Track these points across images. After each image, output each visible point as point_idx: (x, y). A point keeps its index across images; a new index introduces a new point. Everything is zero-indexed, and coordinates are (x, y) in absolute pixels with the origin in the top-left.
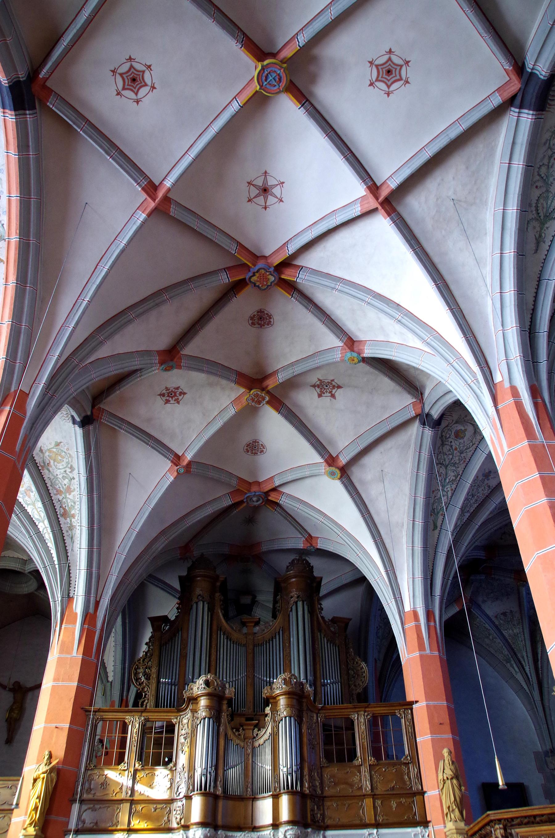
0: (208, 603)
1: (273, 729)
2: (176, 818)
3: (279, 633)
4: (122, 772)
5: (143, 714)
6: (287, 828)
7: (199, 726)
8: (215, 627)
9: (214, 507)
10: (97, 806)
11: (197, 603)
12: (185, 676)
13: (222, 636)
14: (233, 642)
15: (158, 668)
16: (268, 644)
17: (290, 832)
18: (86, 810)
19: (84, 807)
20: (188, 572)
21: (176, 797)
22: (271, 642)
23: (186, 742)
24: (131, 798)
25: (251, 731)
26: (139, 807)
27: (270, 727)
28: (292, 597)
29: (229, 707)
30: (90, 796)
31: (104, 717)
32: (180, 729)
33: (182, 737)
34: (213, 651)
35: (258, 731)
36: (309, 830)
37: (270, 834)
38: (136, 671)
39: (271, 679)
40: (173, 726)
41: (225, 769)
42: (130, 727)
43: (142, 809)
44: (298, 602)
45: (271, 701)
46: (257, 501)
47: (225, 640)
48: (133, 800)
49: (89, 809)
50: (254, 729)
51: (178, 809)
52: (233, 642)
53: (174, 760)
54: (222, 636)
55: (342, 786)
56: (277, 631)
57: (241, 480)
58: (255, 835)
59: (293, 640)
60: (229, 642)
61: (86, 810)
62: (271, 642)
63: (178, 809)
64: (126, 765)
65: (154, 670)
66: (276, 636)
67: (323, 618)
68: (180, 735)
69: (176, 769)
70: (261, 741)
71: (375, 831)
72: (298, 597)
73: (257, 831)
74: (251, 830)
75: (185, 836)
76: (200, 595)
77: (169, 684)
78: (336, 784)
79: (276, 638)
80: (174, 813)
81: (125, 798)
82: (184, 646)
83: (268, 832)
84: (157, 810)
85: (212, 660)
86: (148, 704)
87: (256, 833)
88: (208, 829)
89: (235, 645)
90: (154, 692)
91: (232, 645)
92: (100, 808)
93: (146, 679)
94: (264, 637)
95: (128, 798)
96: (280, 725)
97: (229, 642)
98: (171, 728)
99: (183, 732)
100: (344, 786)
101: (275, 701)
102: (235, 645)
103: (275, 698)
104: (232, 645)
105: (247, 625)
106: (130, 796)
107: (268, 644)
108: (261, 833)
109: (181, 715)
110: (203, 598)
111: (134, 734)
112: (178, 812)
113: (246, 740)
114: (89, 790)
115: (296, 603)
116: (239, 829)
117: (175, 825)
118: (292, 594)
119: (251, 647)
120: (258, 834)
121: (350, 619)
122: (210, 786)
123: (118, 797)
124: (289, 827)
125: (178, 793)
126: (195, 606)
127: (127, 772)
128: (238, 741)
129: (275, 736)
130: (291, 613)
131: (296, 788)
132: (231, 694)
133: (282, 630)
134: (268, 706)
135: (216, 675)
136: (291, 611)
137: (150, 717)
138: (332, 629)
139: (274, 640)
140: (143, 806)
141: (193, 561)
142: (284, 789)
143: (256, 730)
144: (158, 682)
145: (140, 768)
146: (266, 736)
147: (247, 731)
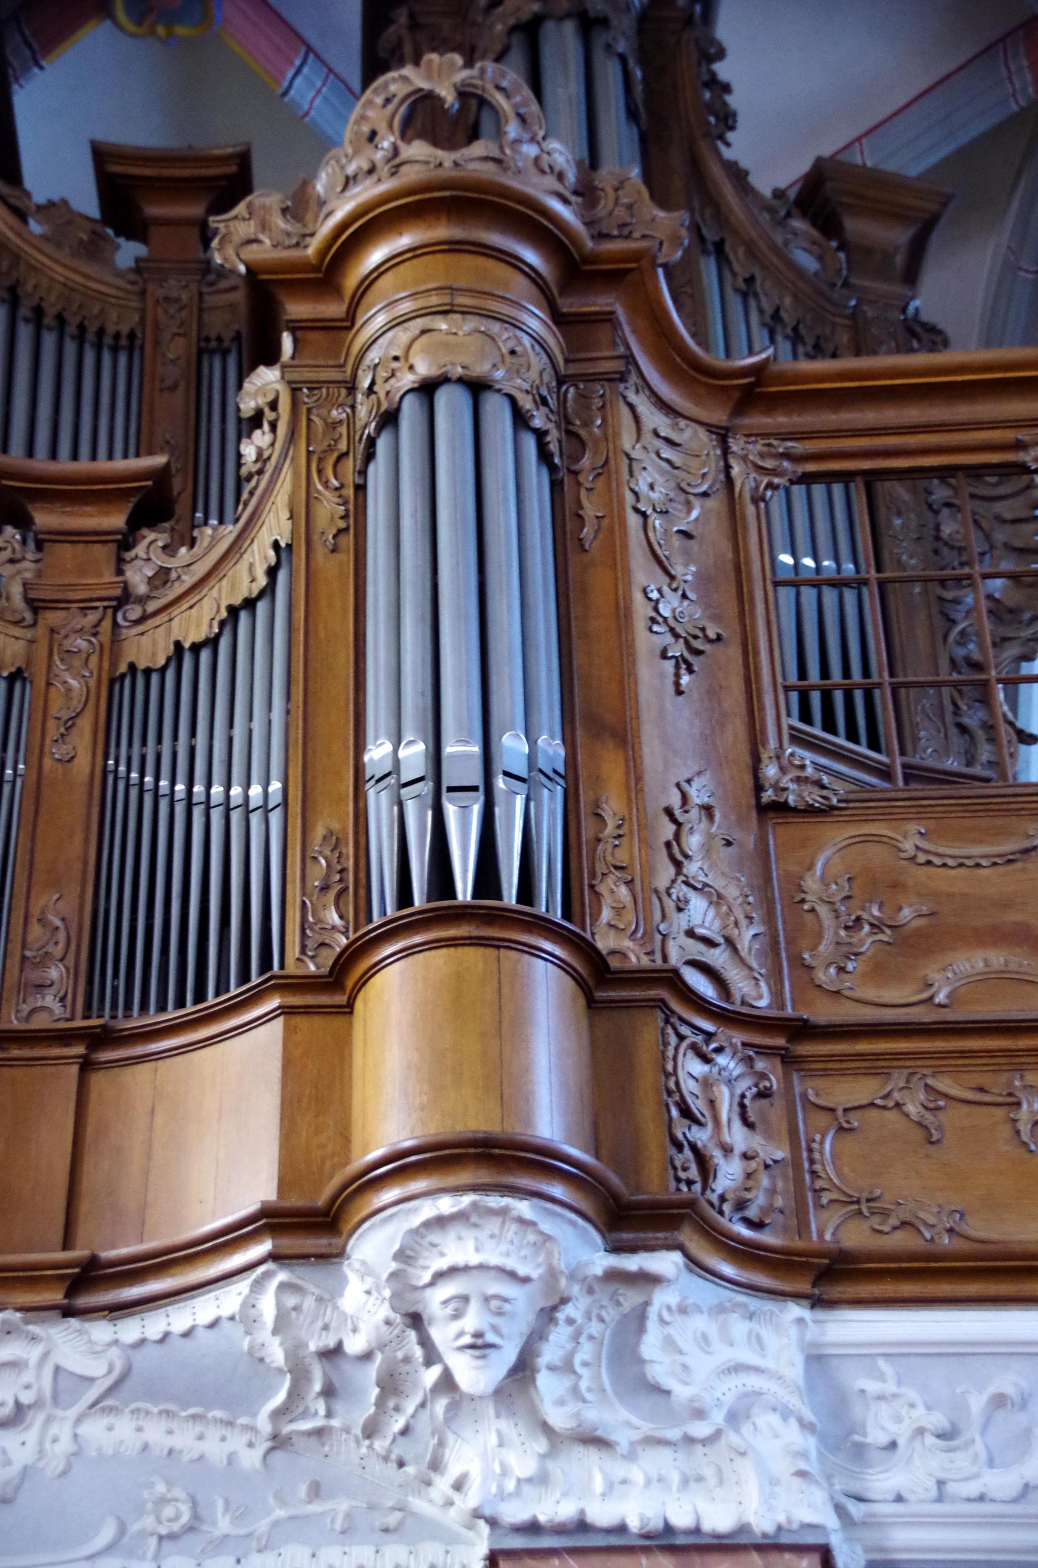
1: (303, 513)
6: (428, 1209)
17: (458, 1249)
25: (104, 553)
35: (169, 549)
36: (665, 1263)
37: (246, 1317)
44: (549, 28)
55: (970, 962)
58: (85, 1347)
67: (738, 175)
74: (57, 1296)
78: (910, 947)
83: (229, 1300)
87: (101, 1331)
89: (49, 341)
96: (378, 473)
100: (997, 958)
101: (333, 309)
102: (49, 341)
103: (326, 273)
105: (154, 210)
108: (153, 1324)
113: (53, 618)
119: (177, 349)
120: (130, 1329)
124: (446, 1205)
129: (328, 562)
134: (270, 356)
138: (808, 262)
142: (404, 897)
146: (247, 575)
147: (66, 553)
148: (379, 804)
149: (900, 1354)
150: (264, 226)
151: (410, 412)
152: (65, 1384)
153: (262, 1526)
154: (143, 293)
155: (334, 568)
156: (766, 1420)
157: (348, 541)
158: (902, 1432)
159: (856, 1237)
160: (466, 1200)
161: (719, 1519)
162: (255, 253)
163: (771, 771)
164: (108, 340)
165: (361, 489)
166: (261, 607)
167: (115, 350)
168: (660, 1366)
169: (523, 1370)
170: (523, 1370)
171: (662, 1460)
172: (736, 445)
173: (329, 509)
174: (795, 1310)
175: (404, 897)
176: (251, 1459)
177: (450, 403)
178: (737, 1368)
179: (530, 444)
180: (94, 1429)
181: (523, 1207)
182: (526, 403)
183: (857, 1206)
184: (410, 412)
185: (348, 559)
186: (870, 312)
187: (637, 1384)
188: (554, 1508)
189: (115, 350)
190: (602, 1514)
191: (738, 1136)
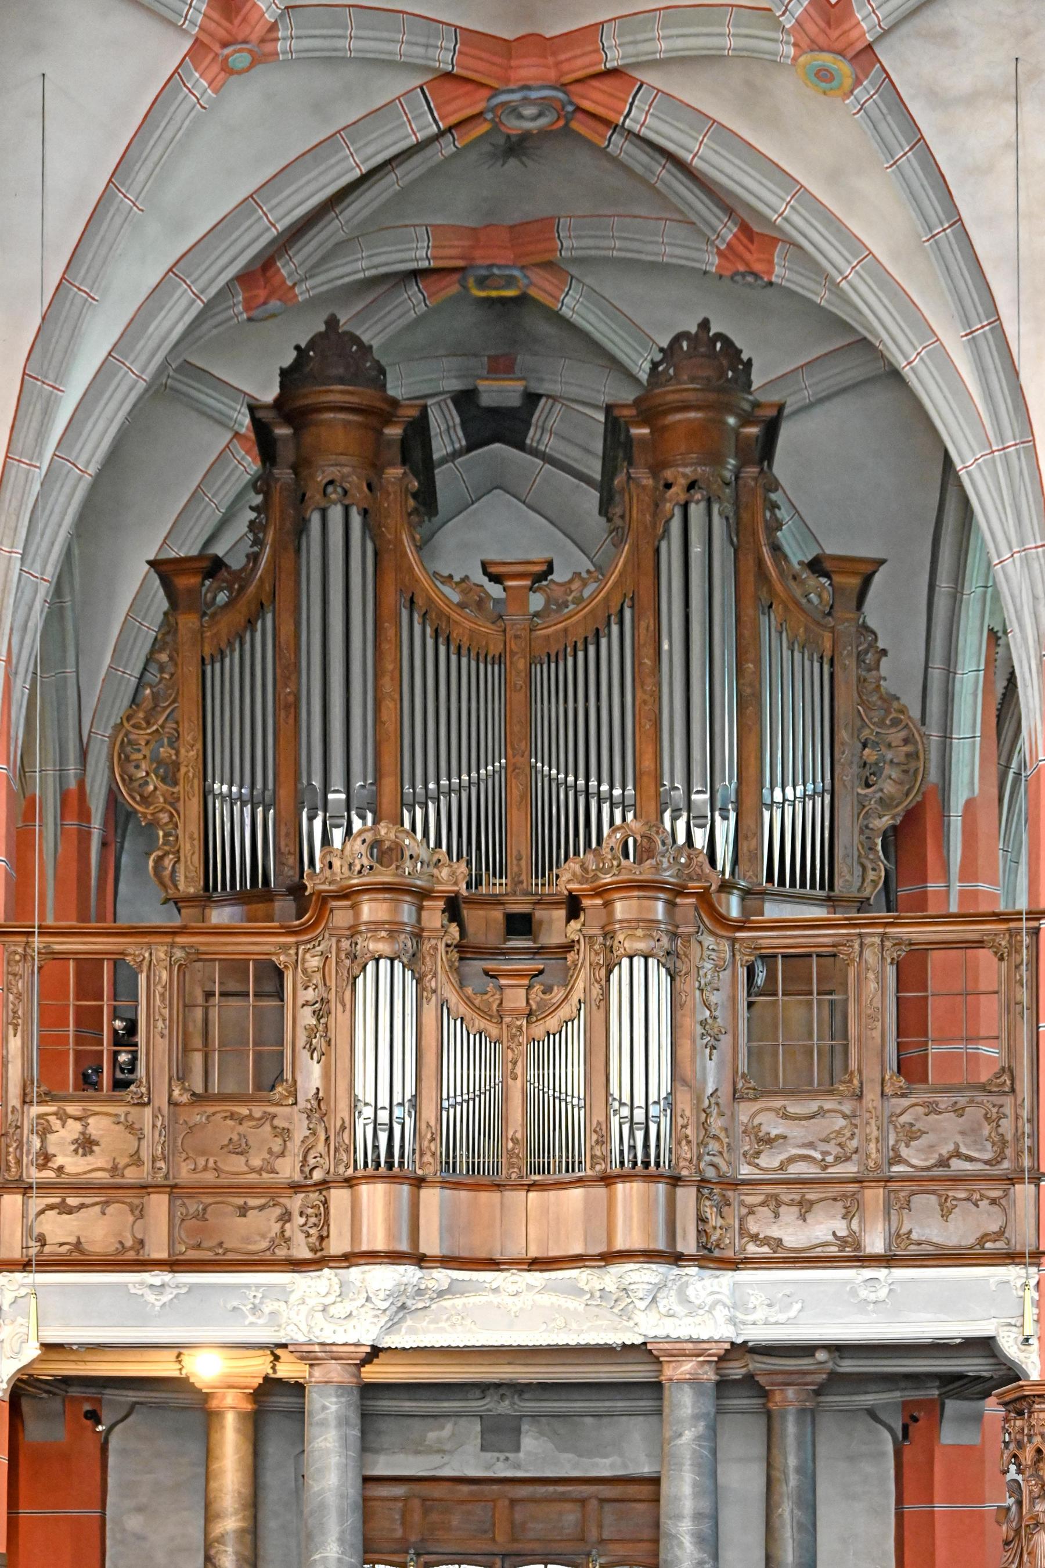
0: (365, 513)
2: (308, 1235)
3: (621, 612)
4: (134, 1110)
5: (179, 940)
7: (360, 981)
8: (390, 597)
9: (370, 150)
10: (72, 1201)
11: (324, 512)
12: (297, 778)
13: (417, 628)
14: (459, 647)
15: (199, 746)
16: (581, 655)
17: (635, 1277)
18: (42, 1212)
19: (36, 1203)
20: (282, 385)
21: (297, 1177)
22: (592, 649)
23: (321, 1028)
24: (171, 1182)
25: (522, 992)
26: (193, 1206)
27: (580, 985)
28: (668, 486)
29: (451, 920)
30: (49, 1175)
31: (57, 948)
32: (299, 986)
33: (308, 1011)
34: (388, 685)
38: (127, 758)
39: (593, 783)
40: (280, 974)
41: (445, 1104)
42: (142, 979)
43: (204, 1210)
44: (693, 507)
45: (586, 902)
46: (534, 118)
47: (430, 642)
48: (175, 1186)
49: (51, 1207)
50: (529, 988)
51: (310, 1211)
52: (459, 647)
53: (288, 1075)
54: (417, 628)
56: (614, 610)
57: (467, 37)
59: (671, 645)
60: (442, 649)
61: (42, 1212)
62: (592, 649)
63: (310, 1211)
64: (144, 1090)
65: (189, 755)
66: (609, 625)
68: (300, 1001)
69: (296, 1103)
70: (552, 1023)
71: (882, 1273)
72: (692, 486)
73: (542, 1271)
75: (335, 1280)
76: (331, 482)
77: (243, 805)
79: (609, 636)
80: (302, 1220)
81: (150, 1180)
82: (289, 669)
84: (250, 1213)
85: (384, 718)
86: (181, 868)
87: (537, 1274)
88: (401, 1269)
90: (194, 827)
91: (454, 658)
92: (82, 1206)
93: (163, 780)
94: (565, 630)
95: (160, 1180)
97: (442, 649)
98: (272, 978)
99: (310, 995)
104: (454, 658)
106: (166, 1177)
107: (581, 655)
109: (297, 944)
110: (346, 492)
111: (158, 1002)
112: (313, 1220)
114: (45, 1159)
115: (685, 507)
116: (491, 1264)
117: (303, 1252)
118: (668, 474)
119: (521, 664)
121: (882, 562)
122: (402, 1147)
123: (131, 1175)
125: (307, 1169)
126: (315, 519)
127: (148, 1111)
128: (481, 1023)
130: (664, 545)
131: (658, 1164)
132: (456, 884)
133: (632, 607)
135: (402, 825)
136: (666, 531)
137: (202, 949)
139: (604, 641)
140: (208, 1200)
141: (297, 348)
143: (537, 988)
144: (206, 793)
145: (185, 1098)
148: (615, 1121)
149: (760, 1284)
150: (574, 874)
151: (625, 962)
152: (530, 1287)
153: (585, 1328)
154: (504, 631)
155: (598, 1016)
156: (719, 1307)
157: (602, 1003)
158: (757, 1303)
159: (752, 1249)
160: (638, 1266)
161: (705, 1338)
162: (570, 886)
163: (740, 1085)
164: (489, 659)
165: (608, 980)
166: (576, 1022)
167: (493, 664)
168: (692, 1298)
169: (654, 1300)
170: (654, 1300)
171: (689, 1320)
172: (737, 946)
173: (596, 990)
174: (730, 1273)
175: (622, 1163)
176: (581, 1308)
177: (638, 962)
178: (713, 1293)
179: (663, 971)
180: (538, 1297)
181: (654, 1266)
182: (663, 960)
183: (754, 1238)
184: (625, 962)
185: (602, 1010)
186: (840, 627)
187: (684, 1300)
188: (661, 1332)
189: (493, 664)
190: (674, 1335)
191: (720, 1222)
